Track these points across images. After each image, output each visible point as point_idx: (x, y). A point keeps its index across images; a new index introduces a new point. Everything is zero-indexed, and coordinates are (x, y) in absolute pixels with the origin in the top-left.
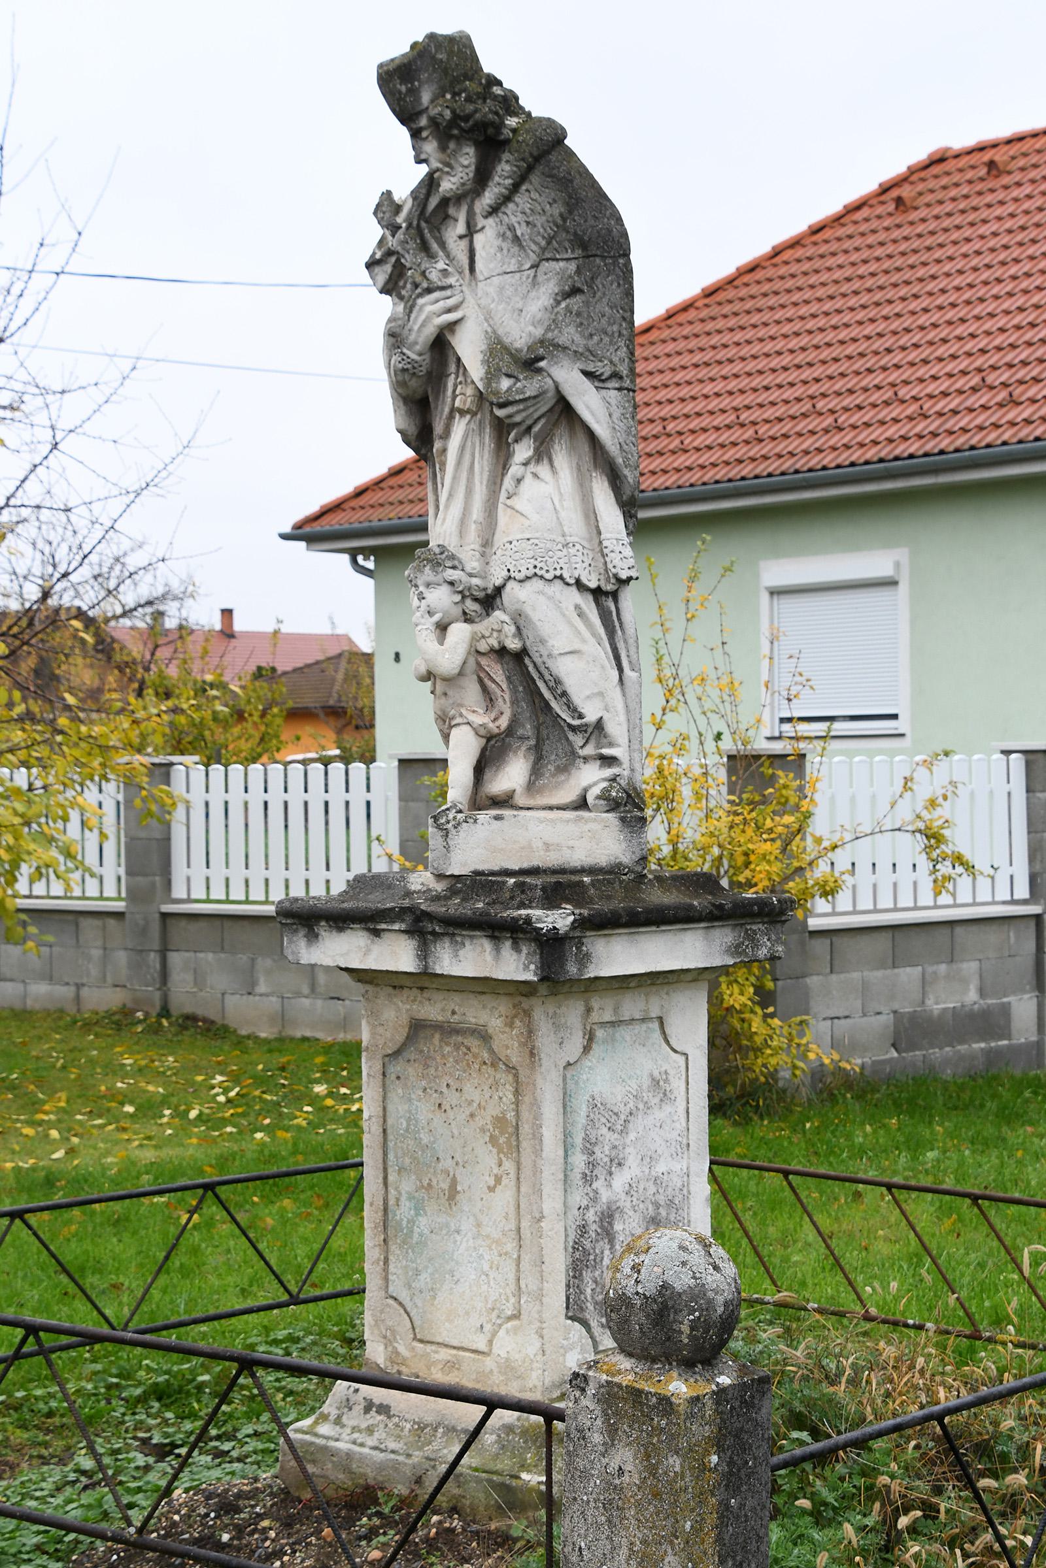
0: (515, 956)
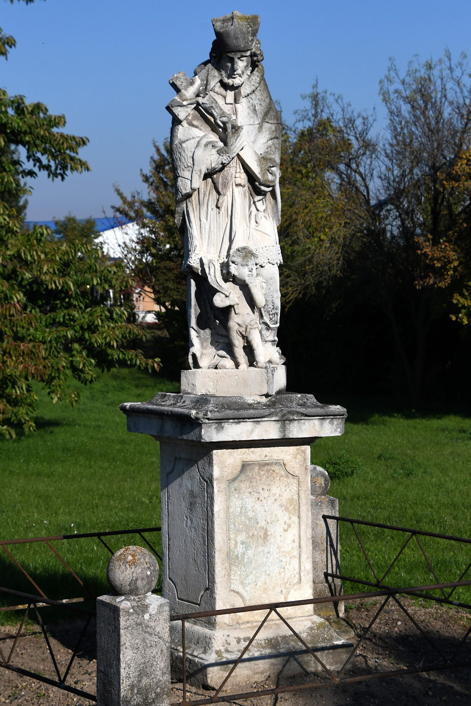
0: (330, 426)
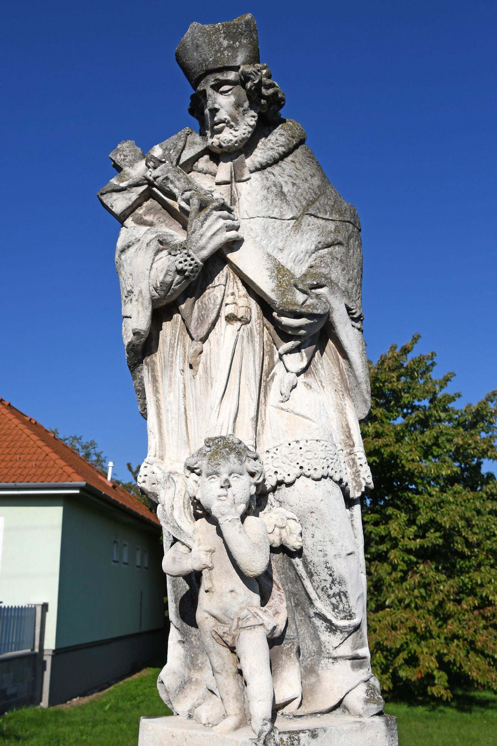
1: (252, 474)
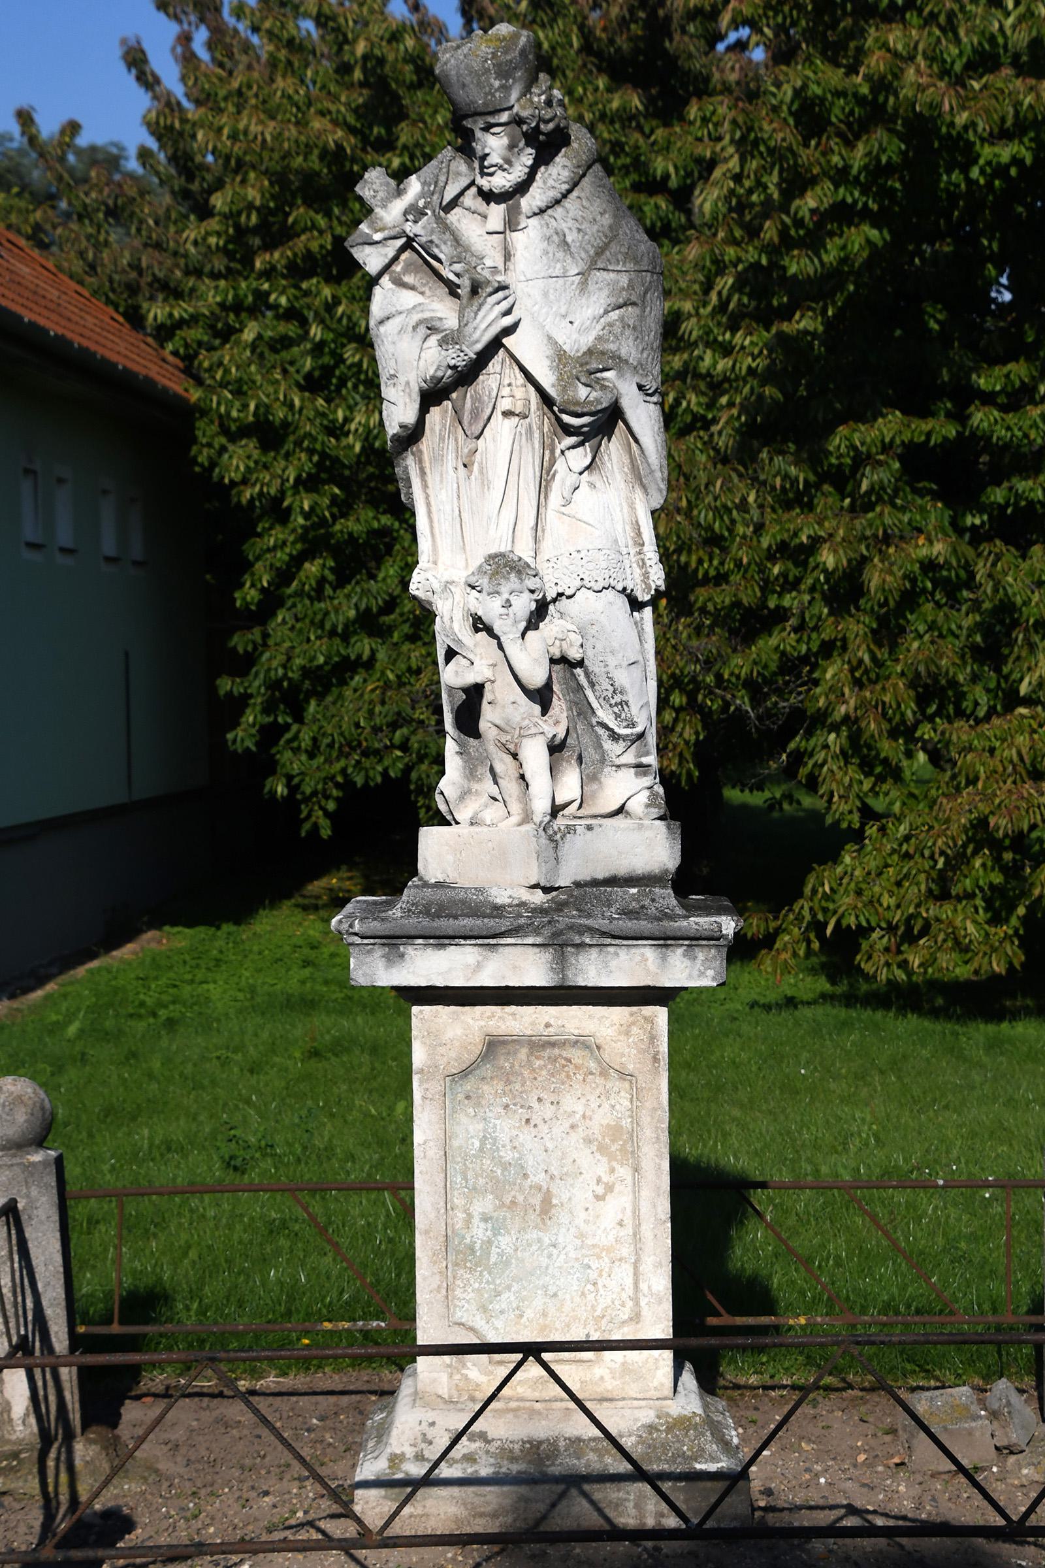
0: (687, 962)
1: (532, 592)
